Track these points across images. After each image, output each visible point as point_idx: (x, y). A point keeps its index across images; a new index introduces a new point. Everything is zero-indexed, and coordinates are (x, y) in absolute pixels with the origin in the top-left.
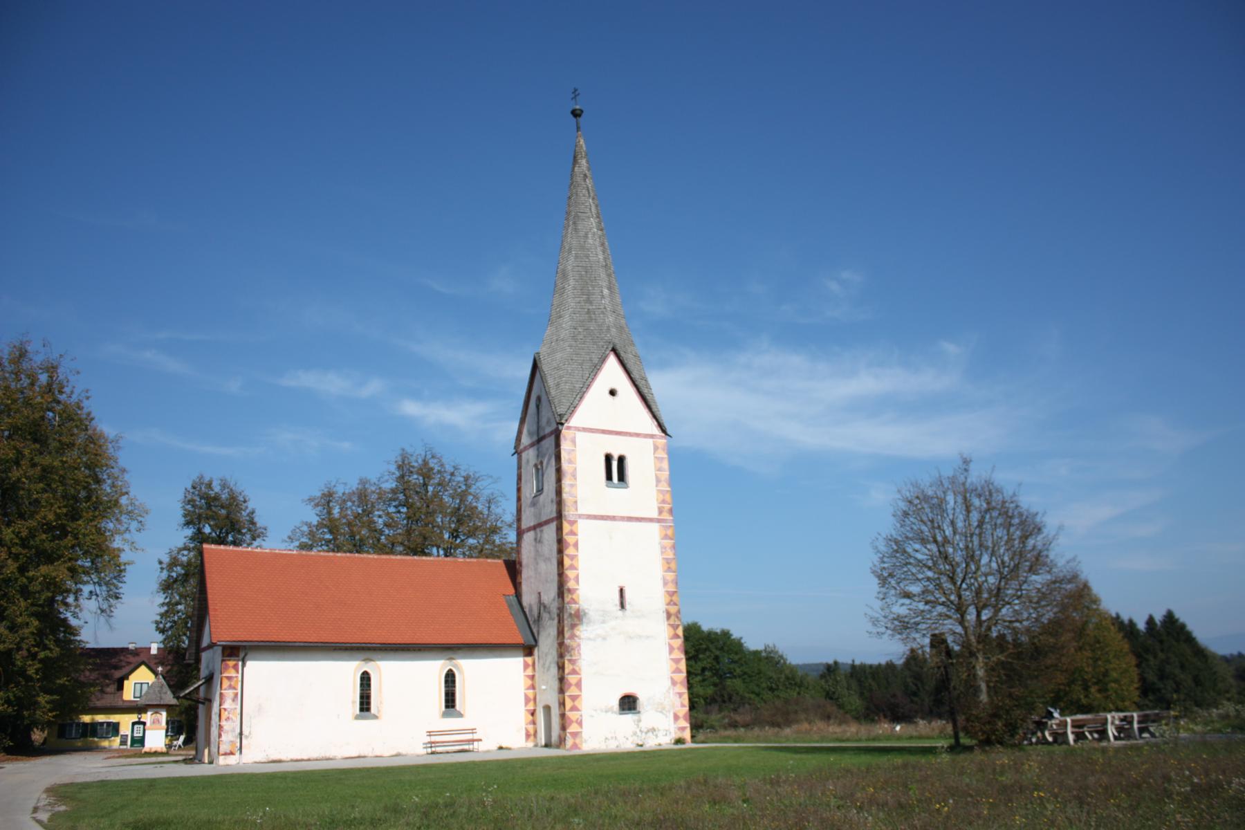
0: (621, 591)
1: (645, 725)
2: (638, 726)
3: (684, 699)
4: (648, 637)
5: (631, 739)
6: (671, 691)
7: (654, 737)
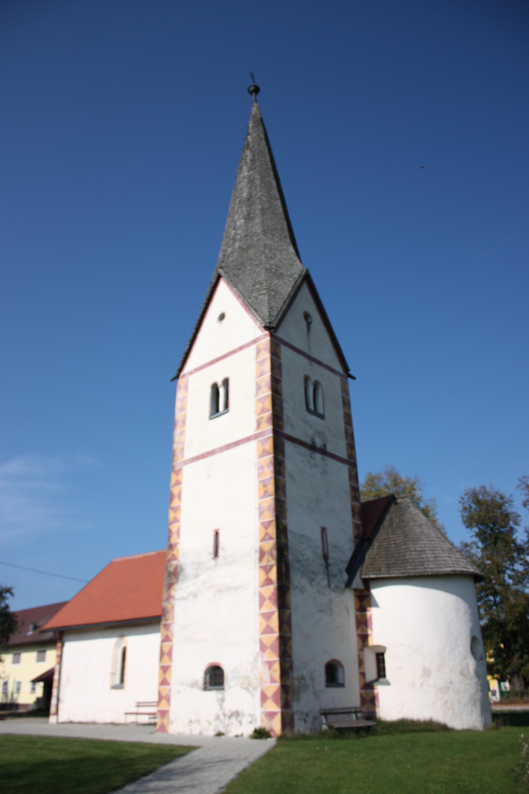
0: (217, 534)
1: (230, 706)
2: (221, 706)
3: (275, 671)
4: (237, 588)
5: (214, 724)
6: (259, 659)
7: (238, 724)
